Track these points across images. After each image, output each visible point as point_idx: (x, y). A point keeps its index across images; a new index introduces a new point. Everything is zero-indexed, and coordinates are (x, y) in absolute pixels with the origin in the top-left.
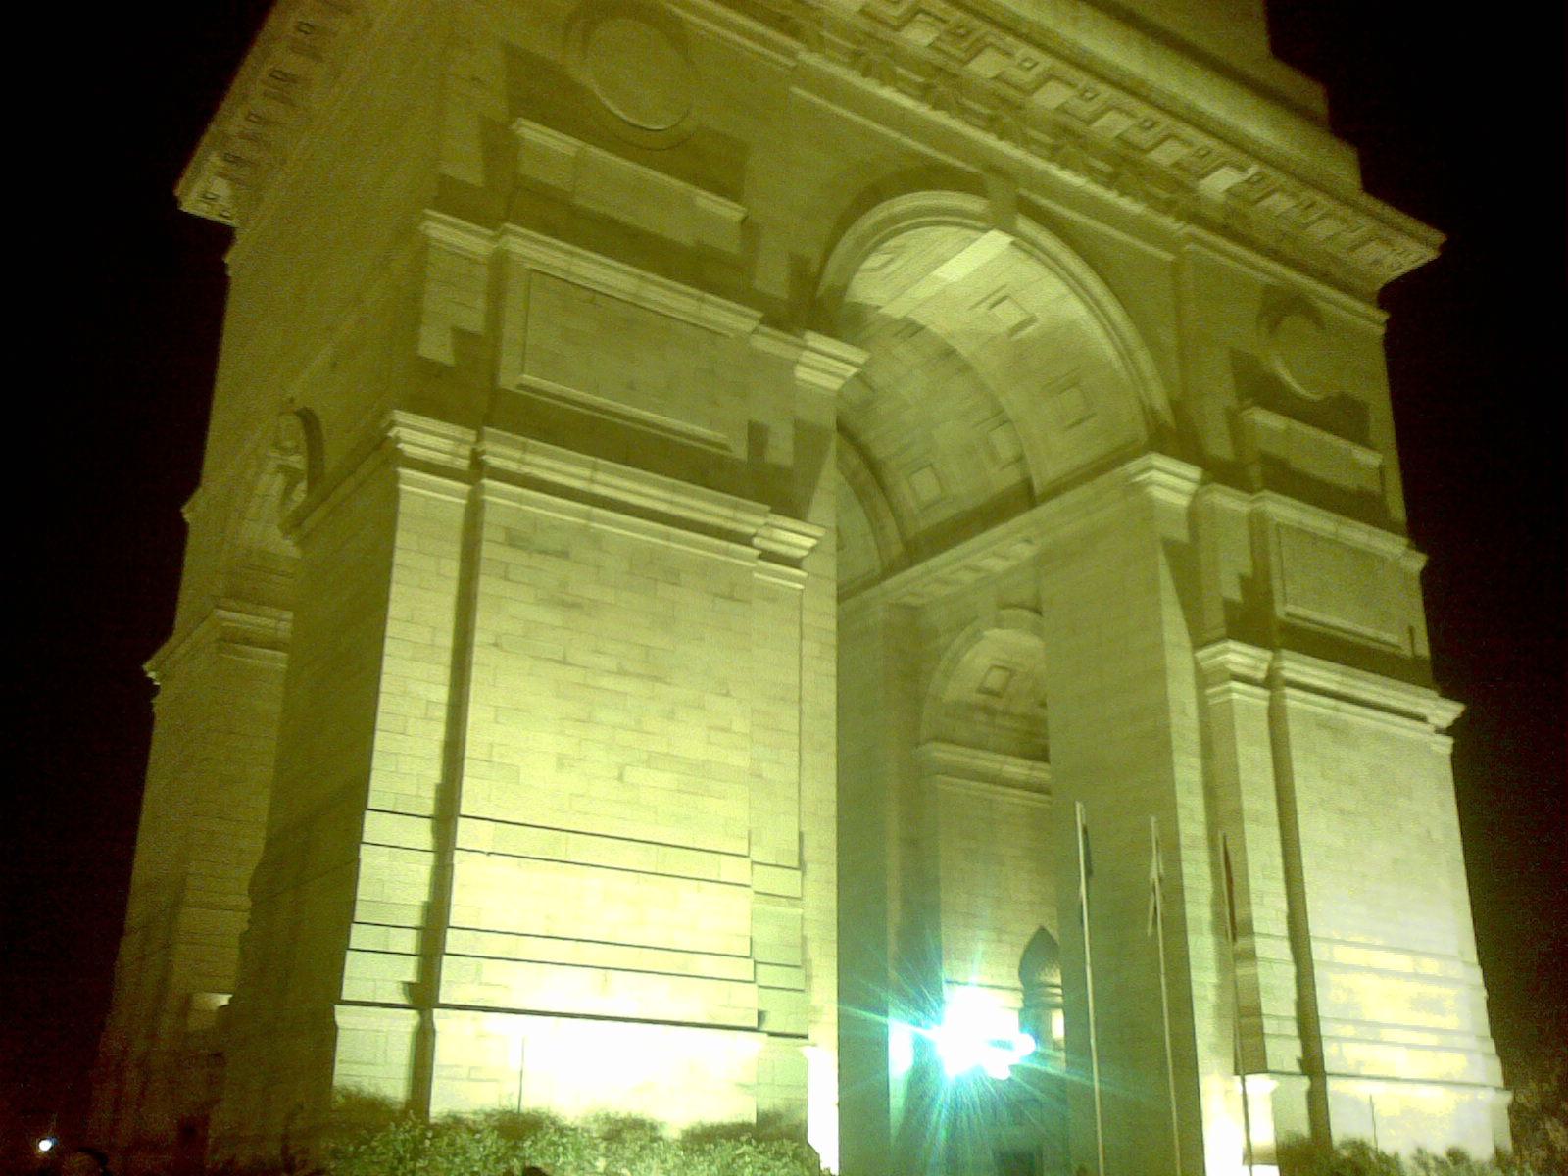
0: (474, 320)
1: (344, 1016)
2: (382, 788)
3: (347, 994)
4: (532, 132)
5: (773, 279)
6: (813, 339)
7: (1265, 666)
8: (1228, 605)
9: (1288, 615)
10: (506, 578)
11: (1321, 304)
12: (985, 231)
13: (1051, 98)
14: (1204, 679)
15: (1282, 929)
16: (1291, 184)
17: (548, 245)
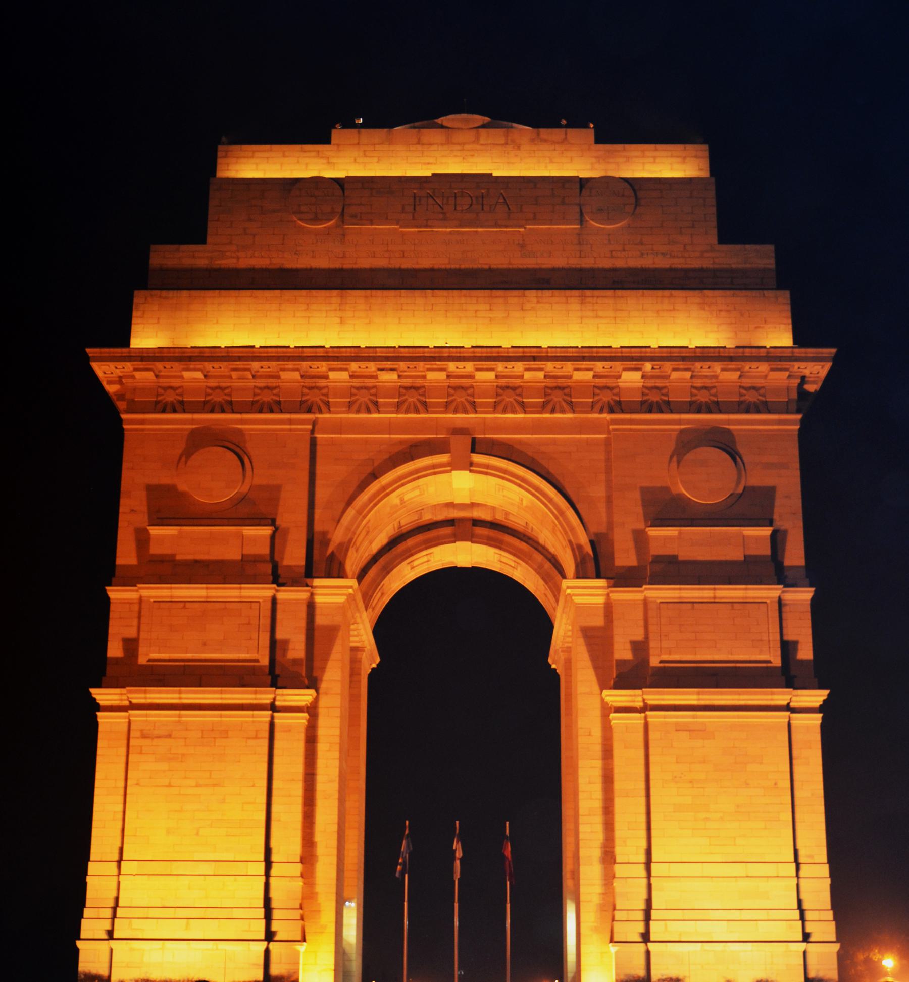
0: (131, 633)
1: (79, 944)
2: (96, 851)
3: (83, 935)
4: (154, 531)
5: (294, 556)
6: (317, 582)
7: (640, 699)
10: (141, 753)
11: (731, 427)
12: (450, 471)
13: (486, 377)
14: (607, 710)
15: (642, 858)
16: (681, 365)
17: (158, 588)
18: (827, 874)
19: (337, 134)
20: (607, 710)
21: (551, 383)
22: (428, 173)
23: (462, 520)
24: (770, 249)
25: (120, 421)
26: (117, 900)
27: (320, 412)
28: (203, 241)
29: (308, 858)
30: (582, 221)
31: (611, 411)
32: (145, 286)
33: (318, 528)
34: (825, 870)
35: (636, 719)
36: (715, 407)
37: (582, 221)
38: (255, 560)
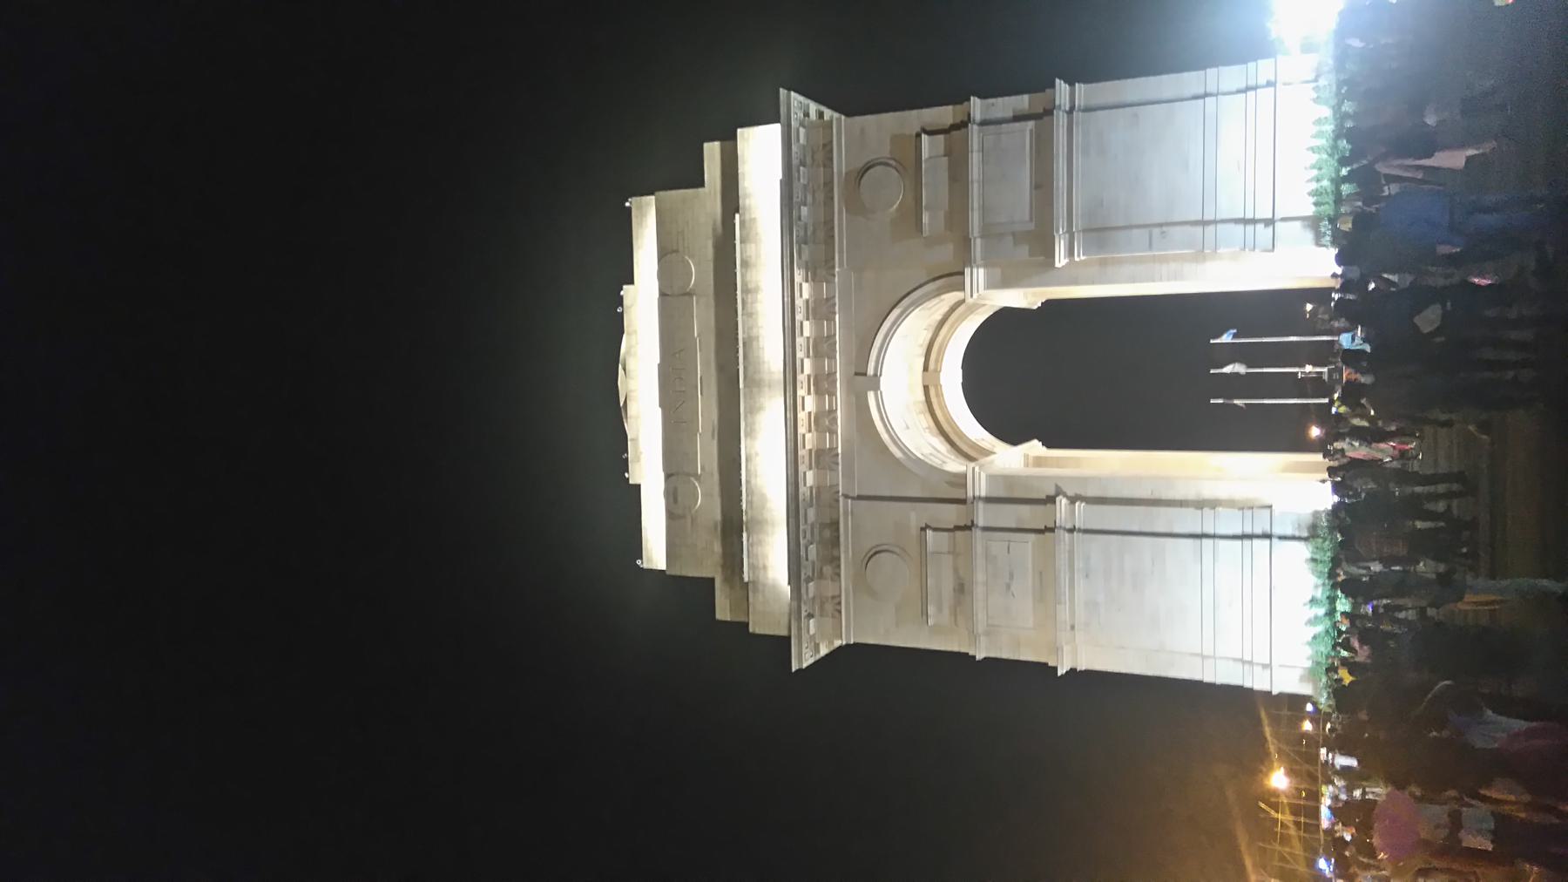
1: (1275, 692)
6: (970, 494)
8: (1031, 255)
15: (1199, 229)
18: (1214, 70)
22: (659, 411)
23: (924, 379)
24: (706, 145)
25: (848, 645)
26: (1235, 660)
28: (712, 580)
30: (690, 294)
32: (747, 625)
36: (829, 184)
37: (690, 294)
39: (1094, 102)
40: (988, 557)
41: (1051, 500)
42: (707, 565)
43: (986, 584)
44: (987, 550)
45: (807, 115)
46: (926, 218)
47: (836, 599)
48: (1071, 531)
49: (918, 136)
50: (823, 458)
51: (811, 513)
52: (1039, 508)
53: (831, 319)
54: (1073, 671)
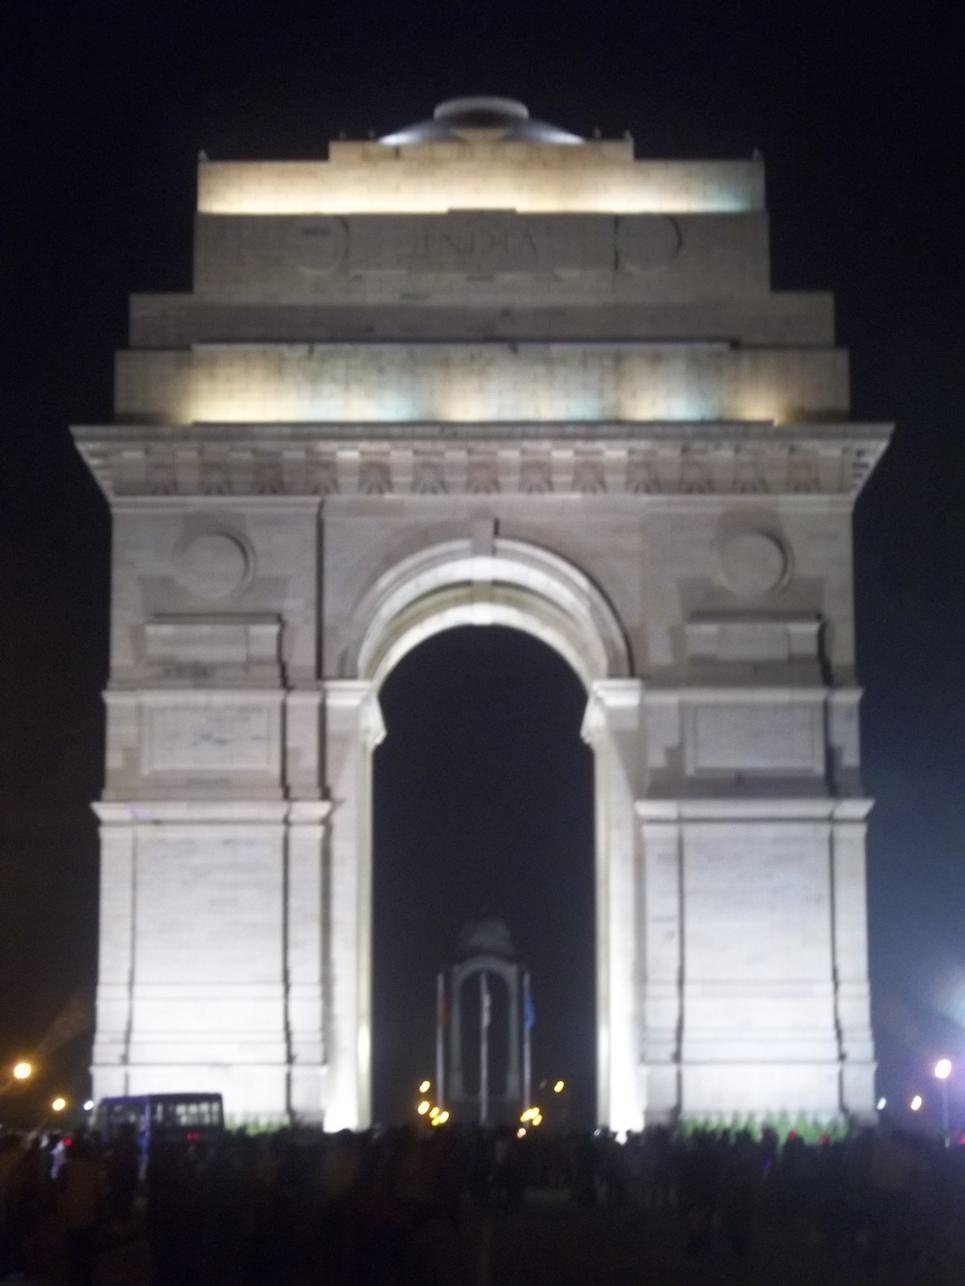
4: (152, 630)
5: (302, 656)
6: (331, 685)
9: (699, 770)
14: (639, 822)
15: (673, 976)
19: (336, 149)
20: (639, 822)
21: (581, 458)
27: (327, 491)
29: (326, 981)
31: (648, 491)
33: (328, 620)
34: (864, 988)
35: (671, 831)
36: (761, 486)
37: (616, 264)
38: (261, 662)
39: (841, 852)
40: (245, 711)
41: (325, 794)
42: (216, 285)
43: (208, 708)
44: (256, 709)
45: (860, 453)
46: (709, 629)
47: (170, 488)
48: (286, 822)
49: (819, 616)
50: (377, 475)
51: (300, 455)
52: (313, 779)
53: (574, 486)
54: (95, 822)
